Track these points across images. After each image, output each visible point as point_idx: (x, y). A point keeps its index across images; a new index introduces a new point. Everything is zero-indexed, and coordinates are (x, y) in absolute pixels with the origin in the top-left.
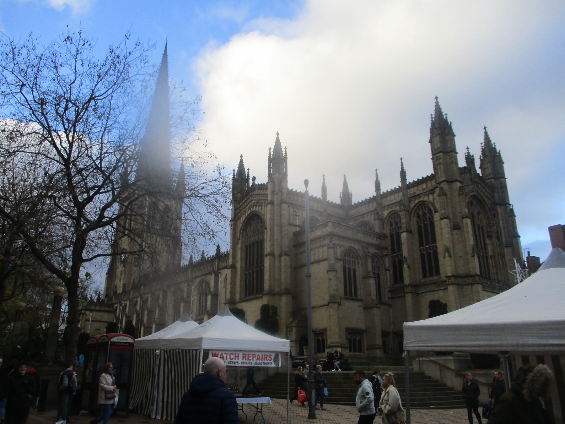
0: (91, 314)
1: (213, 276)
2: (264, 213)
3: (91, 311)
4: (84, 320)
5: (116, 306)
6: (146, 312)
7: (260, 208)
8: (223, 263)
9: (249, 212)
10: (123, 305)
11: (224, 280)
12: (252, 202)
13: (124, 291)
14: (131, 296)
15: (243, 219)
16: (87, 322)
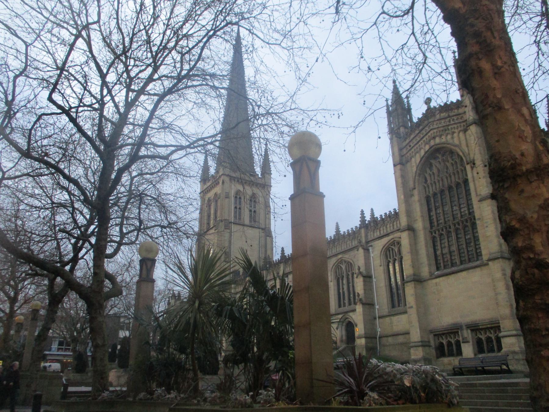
1: (361, 251)
2: (460, 142)
7: (449, 137)
8: (374, 232)
9: (427, 147)
11: (379, 254)
12: (432, 132)
15: (417, 159)
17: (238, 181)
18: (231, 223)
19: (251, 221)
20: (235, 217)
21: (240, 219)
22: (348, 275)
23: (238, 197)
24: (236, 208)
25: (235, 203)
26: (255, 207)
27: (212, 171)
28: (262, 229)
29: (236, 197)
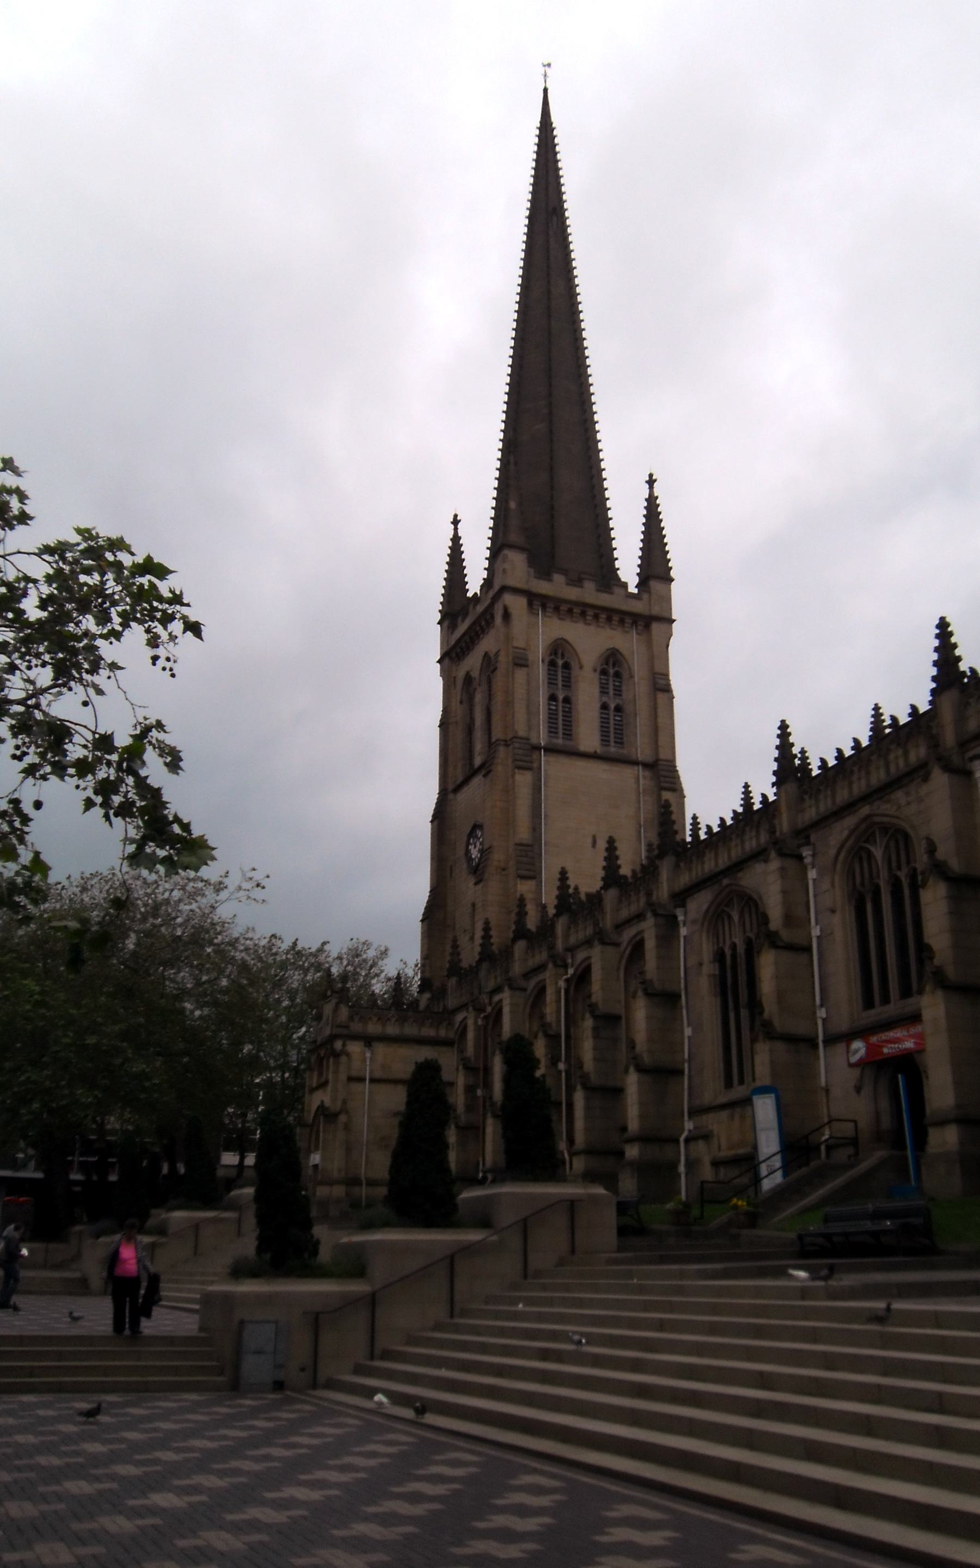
0: (368, 1055)
3: (369, 1041)
4: (343, 1077)
5: (459, 1017)
6: (589, 1023)
10: (489, 1009)
13: (486, 955)
14: (517, 968)
16: (356, 1087)
17: (557, 609)
18: (537, 748)
19: (605, 740)
20: (552, 730)
21: (568, 734)
22: (896, 886)
23: (560, 662)
24: (553, 698)
25: (551, 682)
26: (618, 692)
27: (474, 584)
28: (646, 766)
29: (552, 664)
